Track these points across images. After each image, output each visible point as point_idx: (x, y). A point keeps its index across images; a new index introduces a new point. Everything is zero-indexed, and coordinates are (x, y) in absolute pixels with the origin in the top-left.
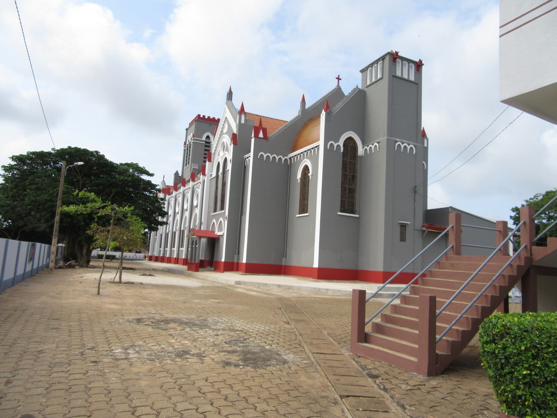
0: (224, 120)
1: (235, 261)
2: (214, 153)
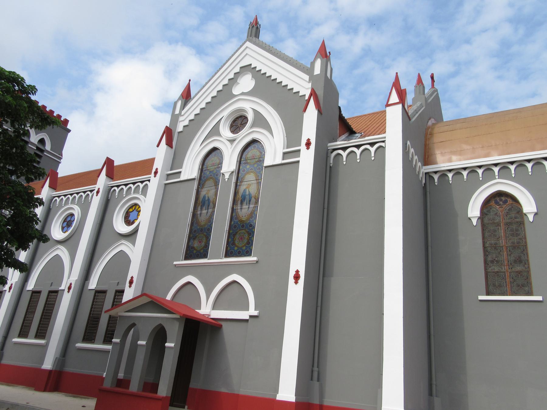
0: (237, 70)
1: (316, 402)
2: (181, 132)
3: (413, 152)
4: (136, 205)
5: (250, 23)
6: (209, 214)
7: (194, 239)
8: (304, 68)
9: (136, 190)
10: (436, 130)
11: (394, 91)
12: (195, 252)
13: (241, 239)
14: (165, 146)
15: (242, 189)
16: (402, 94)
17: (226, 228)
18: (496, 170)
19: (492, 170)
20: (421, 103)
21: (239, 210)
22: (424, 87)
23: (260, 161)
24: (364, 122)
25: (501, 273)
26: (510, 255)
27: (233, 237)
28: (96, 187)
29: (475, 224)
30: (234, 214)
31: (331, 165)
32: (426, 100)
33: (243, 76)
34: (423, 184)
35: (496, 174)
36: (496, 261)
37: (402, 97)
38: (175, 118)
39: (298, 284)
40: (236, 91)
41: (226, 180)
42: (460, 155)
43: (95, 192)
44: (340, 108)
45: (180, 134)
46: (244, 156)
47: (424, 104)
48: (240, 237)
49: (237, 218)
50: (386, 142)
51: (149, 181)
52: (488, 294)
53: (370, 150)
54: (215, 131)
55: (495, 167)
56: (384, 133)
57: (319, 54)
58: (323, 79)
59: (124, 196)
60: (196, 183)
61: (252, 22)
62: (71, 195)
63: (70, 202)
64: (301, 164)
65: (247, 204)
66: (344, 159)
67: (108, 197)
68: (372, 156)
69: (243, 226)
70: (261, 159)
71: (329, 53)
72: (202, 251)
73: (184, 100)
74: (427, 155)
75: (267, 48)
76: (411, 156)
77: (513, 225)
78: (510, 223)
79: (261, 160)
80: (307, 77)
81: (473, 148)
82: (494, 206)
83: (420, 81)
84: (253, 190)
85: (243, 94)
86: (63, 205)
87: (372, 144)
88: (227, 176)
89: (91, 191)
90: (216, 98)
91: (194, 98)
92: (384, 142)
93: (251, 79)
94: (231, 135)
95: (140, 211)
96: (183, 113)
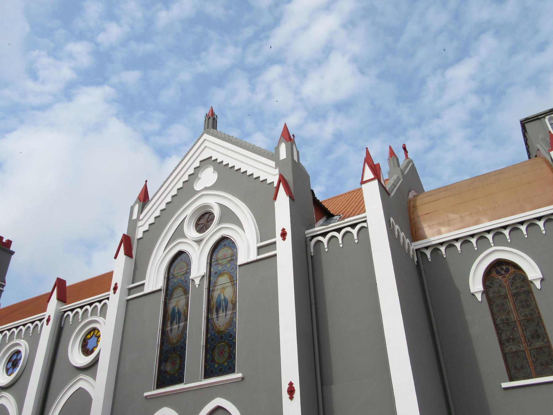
0: (197, 164)
3: (398, 229)
4: (94, 329)
5: (205, 115)
6: (181, 329)
7: (166, 361)
8: (268, 154)
9: (94, 312)
10: (419, 202)
11: (367, 167)
12: (168, 377)
13: (221, 353)
14: (124, 257)
15: (216, 294)
16: (376, 170)
17: (203, 342)
18: (490, 237)
19: (486, 238)
20: (397, 176)
21: (215, 320)
22: (397, 159)
23: (232, 260)
24: (341, 202)
25: (520, 352)
26: (525, 330)
27: (211, 353)
28: (46, 314)
29: (480, 299)
30: (210, 325)
31: (312, 254)
32: (402, 172)
33: (205, 170)
34: (416, 262)
35: (491, 241)
36: (512, 339)
37: (376, 172)
38: (133, 224)
39: (294, 400)
40: (198, 186)
41: (197, 286)
42: (449, 225)
43: (45, 320)
44: (312, 191)
45: (140, 241)
46: (214, 257)
47: (401, 177)
48: (219, 351)
49: (213, 329)
50: (368, 221)
51: (108, 299)
52: (511, 379)
53: (352, 232)
54: (179, 233)
55: (456, 242)
56: (364, 212)
57: (282, 138)
58: (290, 163)
59: (80, 320)
60: (162, 294)
61: (208, 114)
62: (17, 327)
63: (15, 337)
64: (278, 258)
65: (223, 311)
66: (326, 246)
67: (60, 324)
68: (355, 239)
69: (221, 338)
70: (234, 257)
71: (293, 135)
72: (177, 375)
73: (141, 203)
74: (414, 230)
75: (227, 138)
76: (397, 233)
77: (521, 296)
78: (517, 293)
79: (234, 257)
80: (273, 163)
81: (461, 217)
82: (496, 276)
83: (392, 153)
84: (228, 294)
85: (206, 189)
86: (7, 342)
87: (353, 226)
88: (197, 282)
89: (40, 320)
90: (177, 196)
91: (152, 199)
92: (365, 221)
93: (213, 173)
94: (197, 235)
95: (99, 337)
96: (141, 216)
